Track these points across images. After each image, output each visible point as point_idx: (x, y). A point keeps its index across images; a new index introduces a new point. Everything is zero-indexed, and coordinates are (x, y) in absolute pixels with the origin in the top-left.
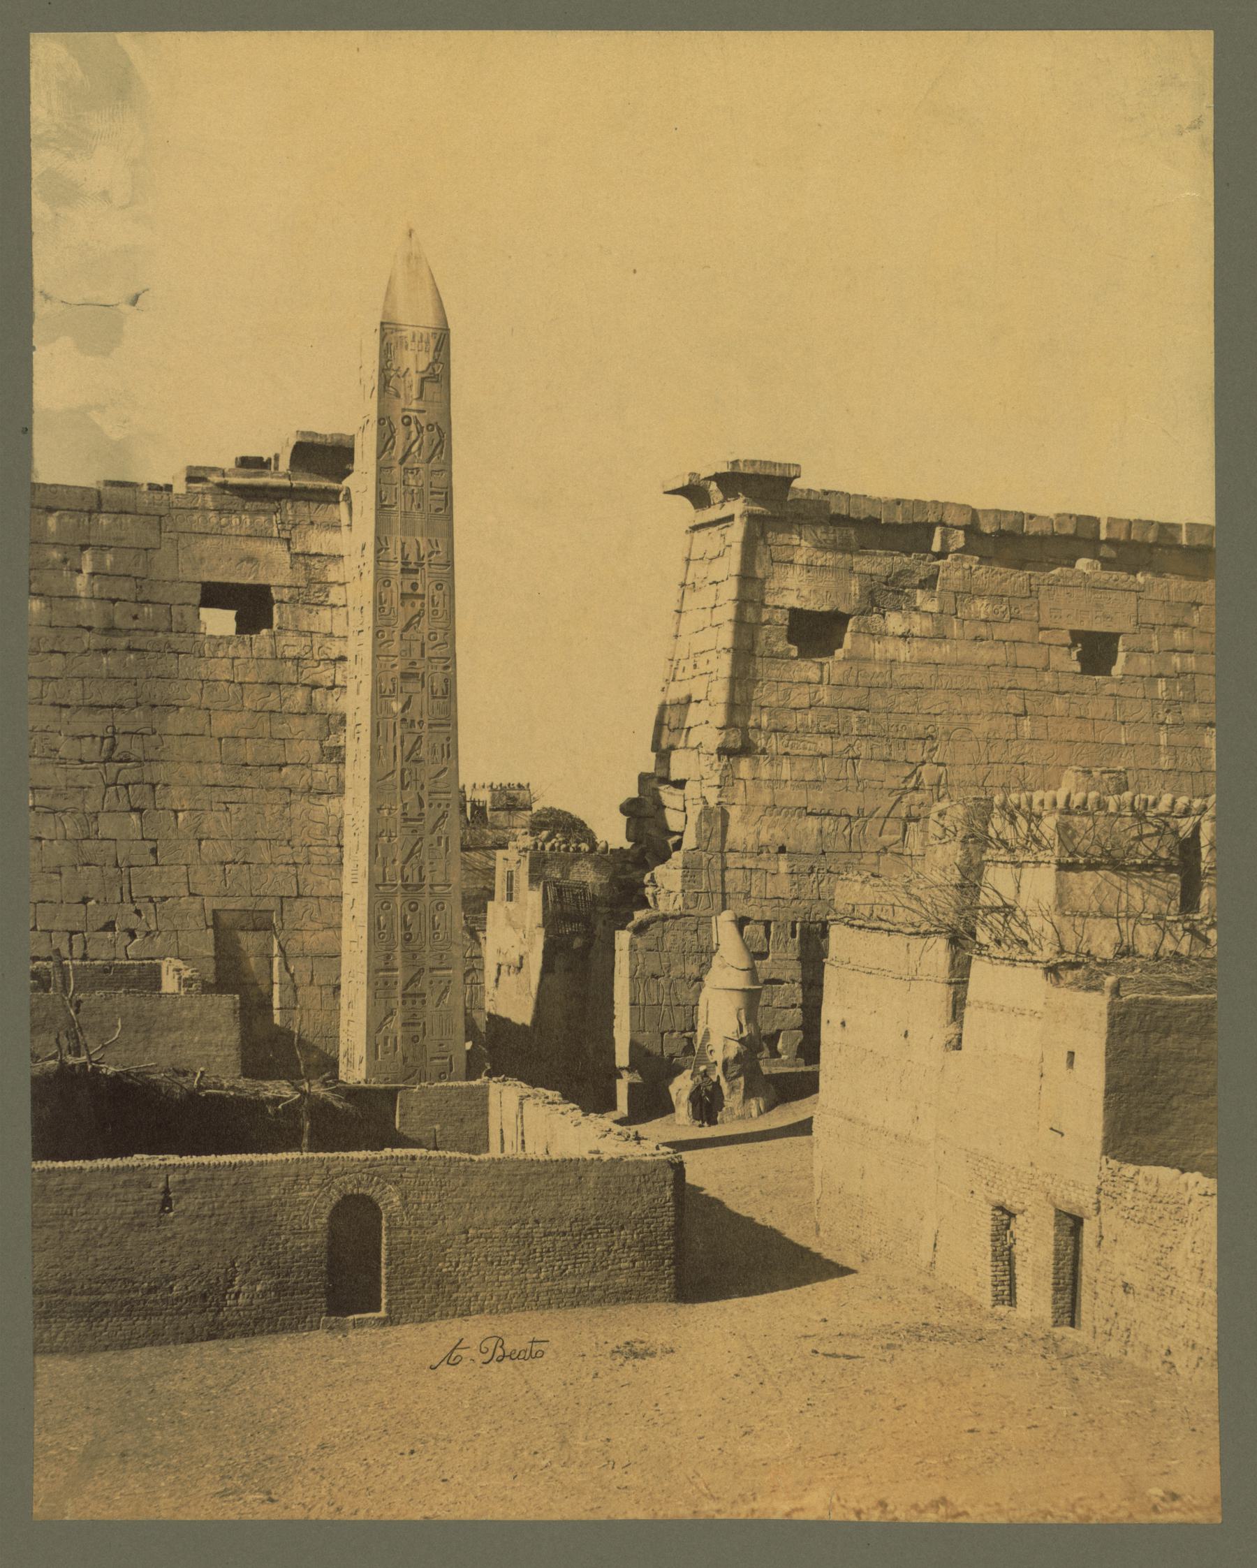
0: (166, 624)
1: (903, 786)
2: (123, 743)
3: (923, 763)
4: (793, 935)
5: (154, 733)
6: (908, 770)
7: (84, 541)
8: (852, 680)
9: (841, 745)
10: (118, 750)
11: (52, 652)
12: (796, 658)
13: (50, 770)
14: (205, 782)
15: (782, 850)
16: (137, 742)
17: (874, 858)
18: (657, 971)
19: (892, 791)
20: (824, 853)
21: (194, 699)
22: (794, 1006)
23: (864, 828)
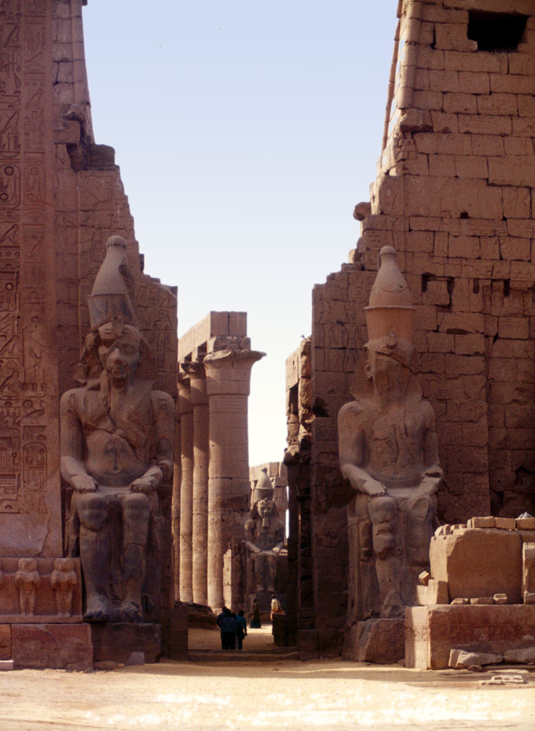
4: (476, 290)
9: (519, 125)
12: (476, 52)
15: (464, 216)
18: (343, 319)
20: (505, 219)
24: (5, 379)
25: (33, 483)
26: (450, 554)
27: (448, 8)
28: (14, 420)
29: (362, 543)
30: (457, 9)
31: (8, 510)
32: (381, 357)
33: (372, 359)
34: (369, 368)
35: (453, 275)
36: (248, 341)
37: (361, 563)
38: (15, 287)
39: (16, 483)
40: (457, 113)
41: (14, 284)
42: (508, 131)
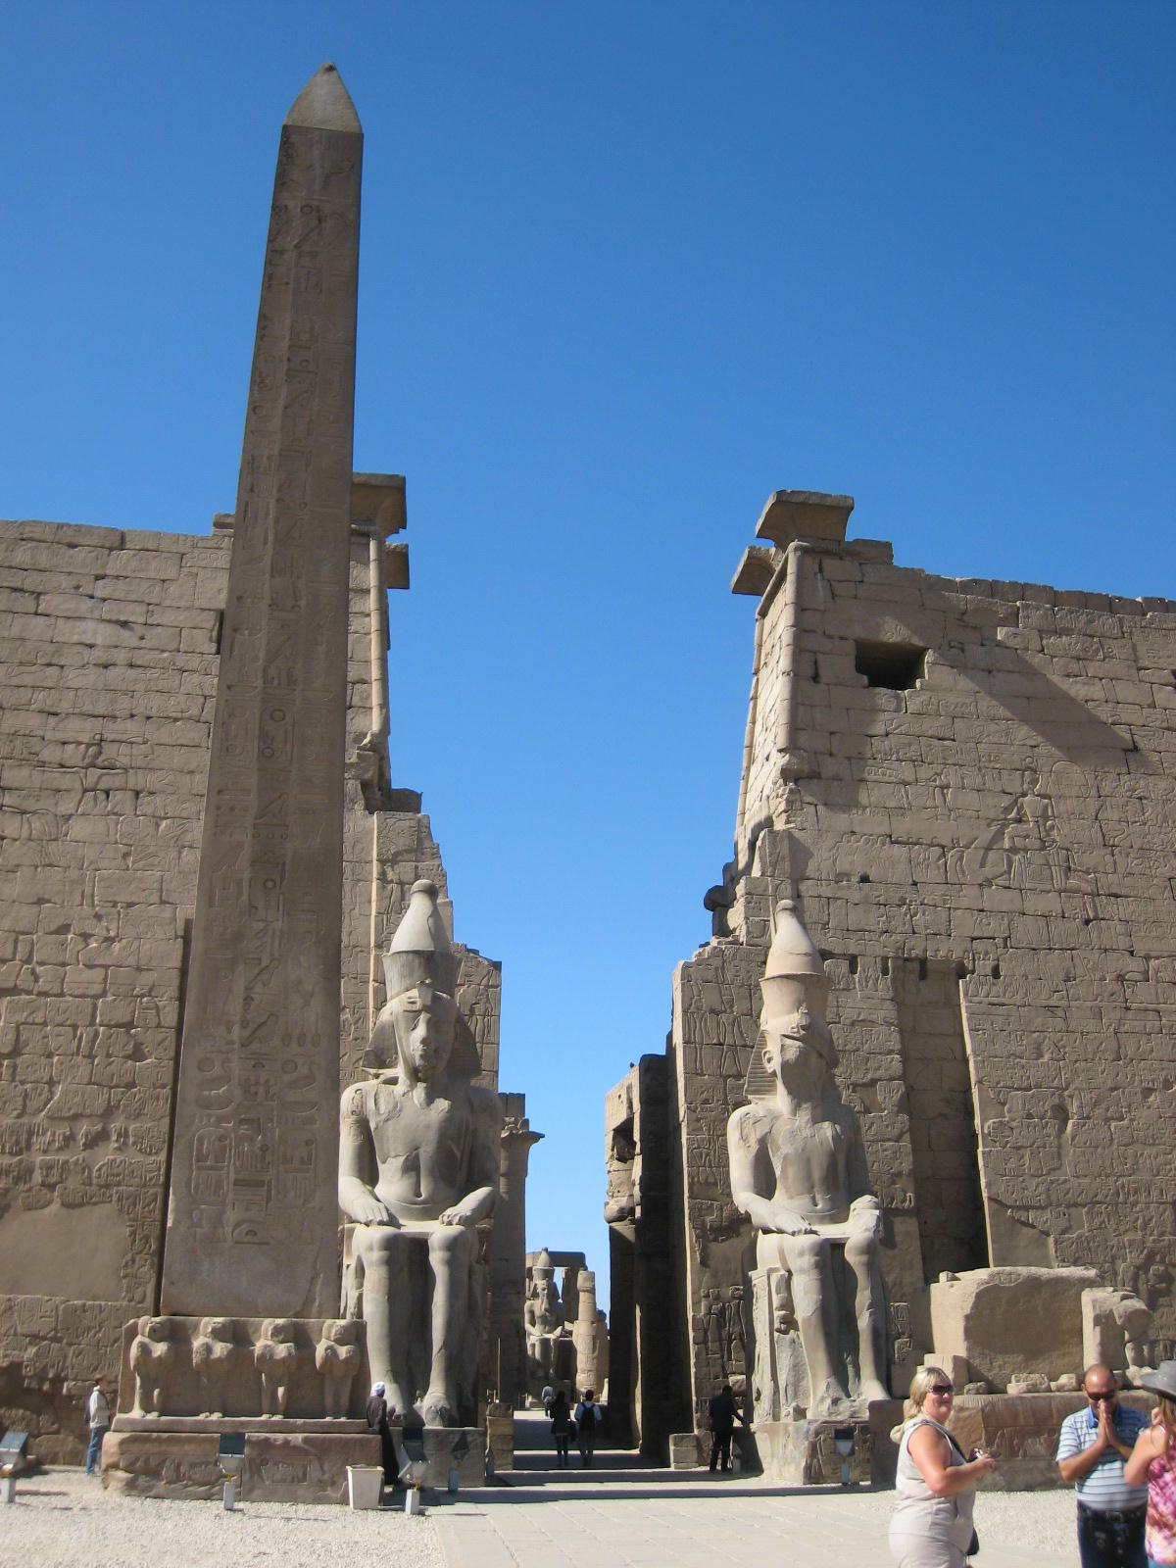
0: (174, 645)
1: (1002, 816)
2: (109, 751)
3: (1024, 795)
4: (885, 972)
5: (145, 743)
6: (1006, 801)
7: (100, 572)
8: (931, 708)
9: (924, 772)
10: (101, 758)
11: (49, 665)
13: (25, 772)
14: (194, 792)
15: (865, 879)
16: (124, 749)
17: (975, 890)
18: (718, 1007)
19: (990, 822)
20: (915, 884)
21: (194, 711)
22: (891, 1052)
23: (961, 859)
24: (255, 1026)
25: (292, 1194)
26: (968, 1311)
27: (830, 637)
28: (267, 1092)
29: (776, 1303)
30: (842, 638)
31: (250, 1238)
32: (789, 1042)
33: (773, 1047)
34: (769, 1060)
35: (856, 953)
36: (526, 1123)
37: (776, 1334)
38: (278, 884)
39: (264, 1194)
40: (849, 758)
41: (278, 879)
42: (911, 778)
